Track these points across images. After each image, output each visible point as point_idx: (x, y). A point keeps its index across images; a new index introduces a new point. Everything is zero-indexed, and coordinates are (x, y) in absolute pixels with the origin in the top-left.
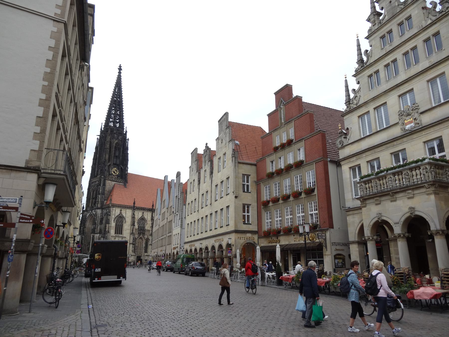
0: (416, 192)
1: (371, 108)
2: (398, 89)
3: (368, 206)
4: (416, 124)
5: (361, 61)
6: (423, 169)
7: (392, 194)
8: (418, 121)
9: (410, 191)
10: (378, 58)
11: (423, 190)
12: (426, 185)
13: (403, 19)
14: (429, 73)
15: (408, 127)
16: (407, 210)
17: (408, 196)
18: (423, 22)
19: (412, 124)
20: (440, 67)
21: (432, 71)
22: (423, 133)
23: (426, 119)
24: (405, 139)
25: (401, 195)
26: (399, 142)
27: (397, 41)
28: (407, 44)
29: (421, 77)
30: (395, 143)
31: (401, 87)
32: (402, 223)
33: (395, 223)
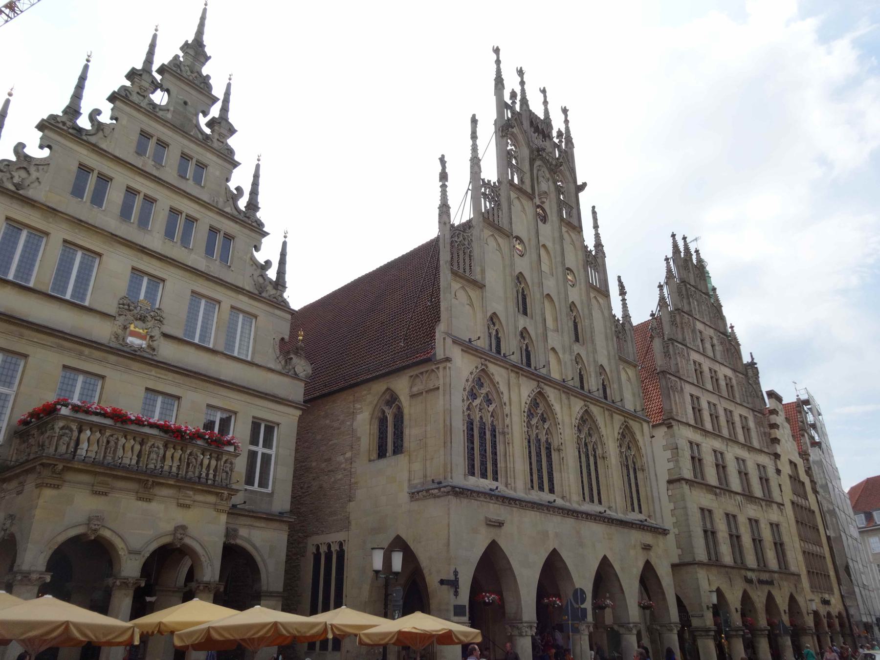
0: (200, 497)
1: (59, 232)
2: (140, 255)
3: (66, 490)
4: (149, 346)
5: (73, 110)
6: (225, 462)
7: (146, 481)
8: (155, 344)
9: (191, 493)
10: (121, 156)
11: (212, 499)
12: (226, 492)
13: (196, 157)
14: (201, 281)
15: (130, 340)
16: (170, 528)
17: (181, 501)
18: (221, 200)
19: (144, 344)
20: (219, 288)
21: (206, 283)
22: (154, 372)
23: (168, 351)
24: (113, 358)
25: (165, 492)
26: (97, 354)
27: (170, 174)
28: (186, 202)
29: (187, 275)
30: (87, 351)
31: (146, 258)
32: (147, 555)
33: (130, 552)
